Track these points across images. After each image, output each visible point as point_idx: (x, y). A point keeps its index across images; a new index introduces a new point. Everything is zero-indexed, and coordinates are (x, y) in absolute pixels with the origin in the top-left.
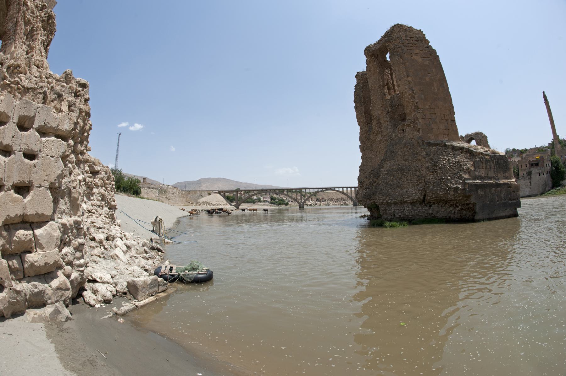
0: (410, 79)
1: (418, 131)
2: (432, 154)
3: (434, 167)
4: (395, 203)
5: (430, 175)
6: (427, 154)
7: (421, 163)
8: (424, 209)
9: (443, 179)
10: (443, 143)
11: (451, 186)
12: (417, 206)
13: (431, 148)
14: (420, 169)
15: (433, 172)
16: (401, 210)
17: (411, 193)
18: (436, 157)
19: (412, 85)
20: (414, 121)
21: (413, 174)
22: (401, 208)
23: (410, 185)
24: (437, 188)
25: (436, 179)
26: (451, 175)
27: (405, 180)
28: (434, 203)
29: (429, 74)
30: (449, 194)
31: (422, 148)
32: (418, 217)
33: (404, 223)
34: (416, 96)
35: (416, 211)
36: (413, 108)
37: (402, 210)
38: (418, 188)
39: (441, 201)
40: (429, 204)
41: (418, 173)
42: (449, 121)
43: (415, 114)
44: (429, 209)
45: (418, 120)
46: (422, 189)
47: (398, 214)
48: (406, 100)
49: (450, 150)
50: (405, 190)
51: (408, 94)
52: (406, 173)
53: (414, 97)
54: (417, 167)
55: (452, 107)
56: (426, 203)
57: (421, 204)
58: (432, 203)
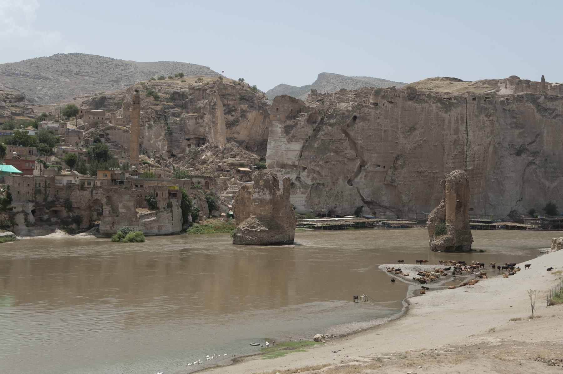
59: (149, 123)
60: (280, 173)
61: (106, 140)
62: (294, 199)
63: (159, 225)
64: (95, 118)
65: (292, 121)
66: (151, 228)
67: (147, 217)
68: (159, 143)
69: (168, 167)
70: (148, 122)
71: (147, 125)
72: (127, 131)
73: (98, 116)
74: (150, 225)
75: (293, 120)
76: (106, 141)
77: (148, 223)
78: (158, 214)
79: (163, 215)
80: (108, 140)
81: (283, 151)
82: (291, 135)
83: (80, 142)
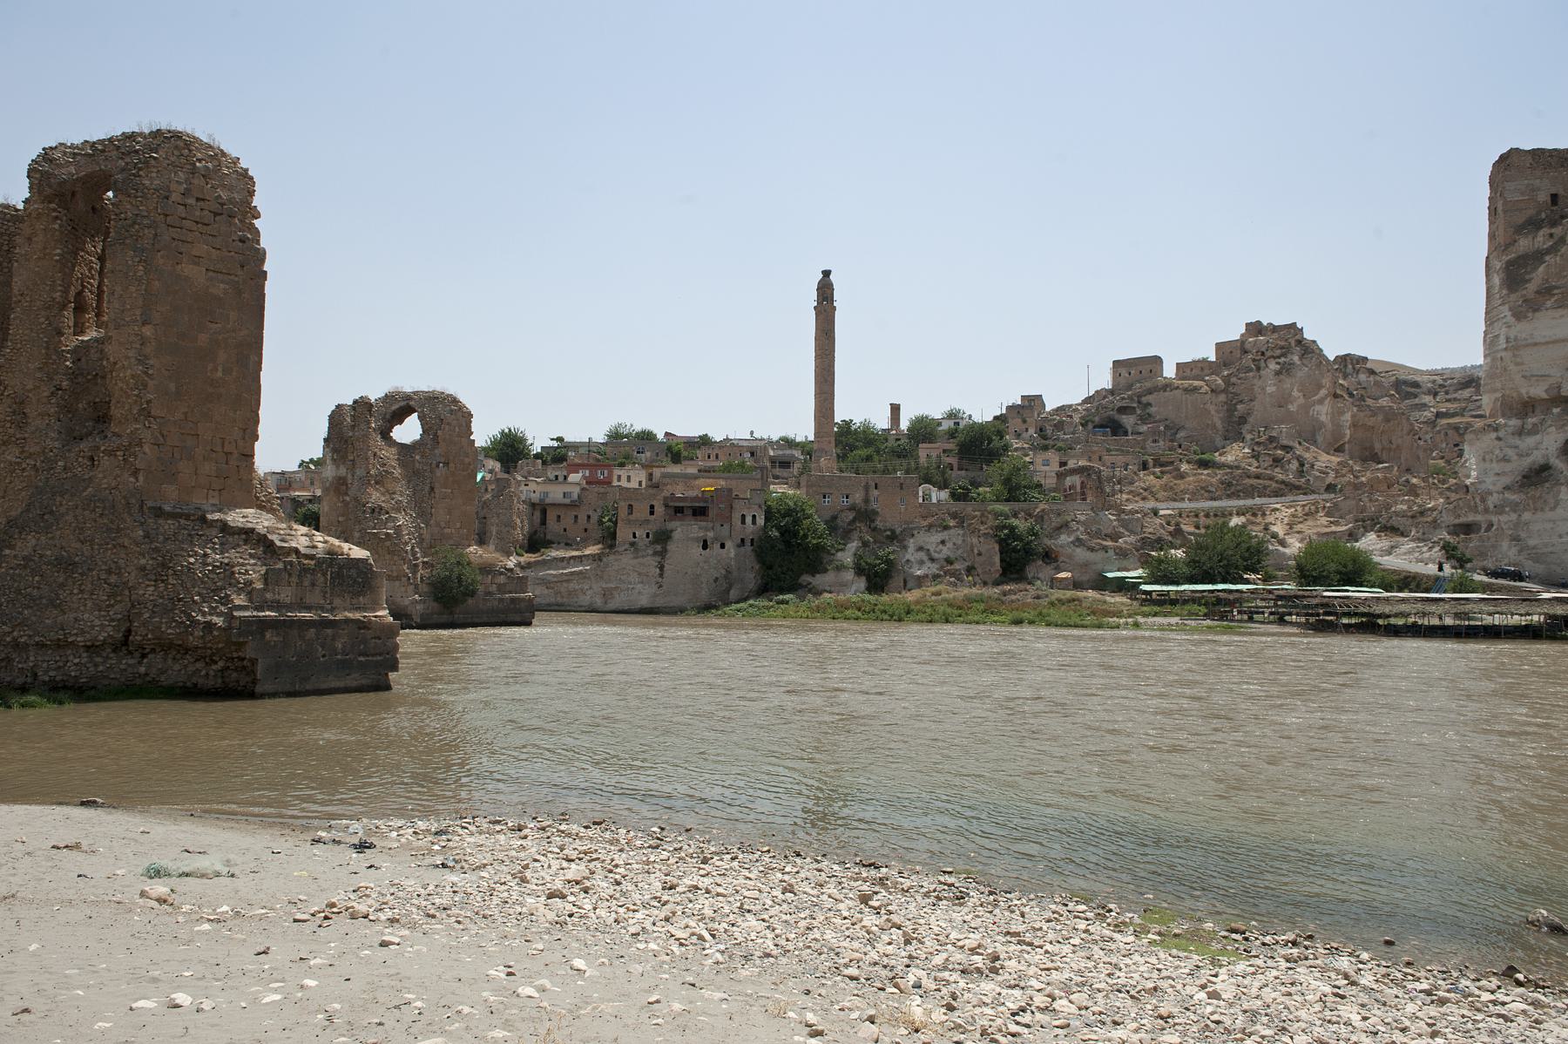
0: (148, 331)
1: (135, 473)
2: (161, 538)
3: (159, 570)
5: (148, 586)
6: (147, 536)
7: (127, 554)
8: (124, 662)
9: (180, 600)
10: (200, 513)
11: (199, 618)
13: (161, 521)
14: (120, 569)
15: (155, 581)
16: (56, 662)
18: (170, 546)
19: (148, 350)
20: (129, 445)
22: (58, 658)
23: (89, 604)
24: (161, 619)
25: (161, 597)
27: (75, 591)
30: (192, 635)
32: (106, 682)
33: (61, 695)
34: (151, 383)
35: (101, 668)
36: (135, 412)
37: (61, 664)
38: (111, 613)
39: (166, 646)
40: (140, 651)
41: (113, 579)
42: (236, 455)
43: (137, 429)
44: (140, 663)
45: (142, 447)
46: (119, 616)
47: (46, 672)
48: (120, 384)
50: (72, 616)
51: (129, 372)
53: (145, 386)
54: (116, 563)
58: (148, 650)
59: (1283, 359)
60: (1494, 435)
62: (1549, 526)
65: (1541, 233)
67: (560, 564)
68: (1317, 408)
69: (1282, 467)
70: (1279, 357)
71: (1273, 366)
72: (1196, 389)
73: (1140, 368)
74: (565, 584)
75: (1545, 231)
78: (605, 560)
79: (616, 560)
80: (1145, 419)
81: (1503, 354)
82: (1532, 287)
83: (1027, 430)
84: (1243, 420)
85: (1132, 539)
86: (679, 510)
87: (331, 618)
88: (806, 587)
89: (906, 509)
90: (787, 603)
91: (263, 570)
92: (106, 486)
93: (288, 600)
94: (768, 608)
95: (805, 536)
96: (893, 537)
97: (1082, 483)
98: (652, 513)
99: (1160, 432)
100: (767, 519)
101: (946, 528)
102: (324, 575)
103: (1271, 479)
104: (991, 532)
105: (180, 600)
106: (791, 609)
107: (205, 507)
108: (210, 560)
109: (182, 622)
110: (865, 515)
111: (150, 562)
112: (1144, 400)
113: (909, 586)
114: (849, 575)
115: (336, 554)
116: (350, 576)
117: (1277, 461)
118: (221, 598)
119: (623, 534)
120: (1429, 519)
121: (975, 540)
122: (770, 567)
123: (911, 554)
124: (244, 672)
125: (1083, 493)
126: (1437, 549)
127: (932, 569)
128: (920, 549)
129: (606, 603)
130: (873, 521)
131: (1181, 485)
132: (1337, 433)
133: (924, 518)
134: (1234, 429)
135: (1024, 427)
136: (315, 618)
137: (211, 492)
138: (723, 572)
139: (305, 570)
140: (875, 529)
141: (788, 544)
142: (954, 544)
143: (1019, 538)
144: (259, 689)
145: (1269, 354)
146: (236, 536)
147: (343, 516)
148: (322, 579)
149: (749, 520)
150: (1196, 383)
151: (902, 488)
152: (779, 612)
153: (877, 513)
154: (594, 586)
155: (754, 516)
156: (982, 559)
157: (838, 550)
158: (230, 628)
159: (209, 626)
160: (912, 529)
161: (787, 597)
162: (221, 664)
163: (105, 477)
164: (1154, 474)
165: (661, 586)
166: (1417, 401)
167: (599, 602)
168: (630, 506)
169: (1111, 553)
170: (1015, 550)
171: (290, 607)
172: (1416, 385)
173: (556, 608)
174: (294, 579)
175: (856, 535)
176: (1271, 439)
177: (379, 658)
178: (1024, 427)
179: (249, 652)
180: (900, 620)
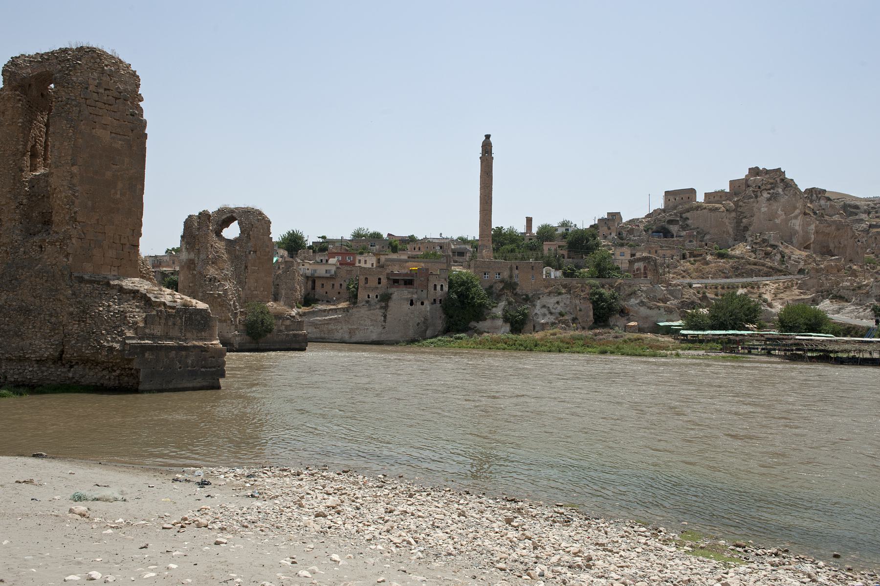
0: (75, 169)
1: (67, 256)
3: (81, 314)
4: (9, 360)
5: (74, 324)
6: (74, 294)
8: (59, 370)
11: (105, 344)
12: (48, 365)
13: (82, 285)
14: (58, 314)
15: (79, 321)
16: (19, 370)
17: (38, 347)
19: (75, 181)
21: (45, 320)
22: (19, 367)
23: (39, 335)
25: (82, 331)
26: (109, 328)
28: (77, 363)
29: (115, 166)
30: (100, 354)
31: (67, 285)
33: (21, 390)
34: (77, 202)
35: (45, 374)
36: (67, 218)
37: (21, 371)
39: (85, 361)
40: (69, 363)
41: (53, 320)
42: (128, 245)
43: (68, 229)
44: (69, 371)
46: (57, 342)
48: (58, 202)
49: (114, 292)
50: (28, 342)
52: (34, 317)
53: (73, 203)
54: (55, 310)
55: (140, 225)
56: (63, 362)
57: (54, 363)
58: (73, 363)
59: (772, 191)
61: (682, 228)
63: (350, 327)
64: (677, 198)
66: (329, 331)
67: (323, 313)
68: (793, 221)
69: (770, 258)
70: (769, 190)
71: (766, 195)
72: (717, 209)
74: (326, 326)
76: (681, 229)
77: (320, 323)
78: (350, 311)
79: (358, 311)
80: (685, 227)
83: (611, 234)
84: (746, 229)
85: (675, 302)
86: (396, 281)
87: (185, 344)
88: (473, 329)
89: (535, 282)
90: (462, 339)
91: (144, 315)
92: (49, 263)
93: (159, 334)
94: (450, 342)
95: (473, 298)
96: (527, 299)
97: (645, 267)
98: (379, 283)
99: (693, 236)
100: (450, 287)
101: (560, 294)
102: (181, 318)
103: (764, 265)
104: (588, 297)
105: (93, 333)
106: (464, 342)
107: (109, 277)
108: (112, 309)
109: (95, 347)
110: (510, 286)
111: (76, 310)
112: (684, 216)
113: (537, 329)
114: (500, 322)
115: (188, 306)
116: (196, 320)
117: (767, 254)
118: (118, 332)
119: (362, 295)
120: (864, 291)
121: (577, 302)
122: (451, 317)
123: (538, 310)
124: (132, 377)
125: (645, 273)
126: (869, 310)
127: (552, 319)
128: (544, 306)
129: (351, 337)
130: (515, 289)
131: (707, 268)
132: (806, 237)
133: (546, 287)
134: (741, 234)
135: (609, 232)
136: (175, 344)
137: (112, 267)
138: (423, 319)
139: (169, 316)
140: (516, 294)
141: (463, 303)
142: (565, 304)
143: (605, 301)
144: (141, 387)
145: (763, 187)
146: (128, 295)
147: (192, 283)
148: (180, 321)
149: (439, 288)
150: (717, 205)
151: (533, 269)
152: (456, 345)
153: (517, 284)
154: (344, 327)
155: (442, 286)
156: (582, 313)
157: (493, 307)
158: (124, 350)
159: (111, 349)
160: (539, 294)
161: (462, 335)
162: (118, 372)
163: (48, 258)
164: (690, 261)
165: (384, 328)
166: (857, 217)
167: (346, 337)
168: (366, 279)
169: (662, 310)
170: (602, 308)
171: (160, 338)
172: (857, 207)
173: (322, 340)
174: (163, 321)
175: (504, 297)
176: (764, 241)
177: (214, 369)
178: (609, 232)
179: (135, 365)
180: (531, 350)
